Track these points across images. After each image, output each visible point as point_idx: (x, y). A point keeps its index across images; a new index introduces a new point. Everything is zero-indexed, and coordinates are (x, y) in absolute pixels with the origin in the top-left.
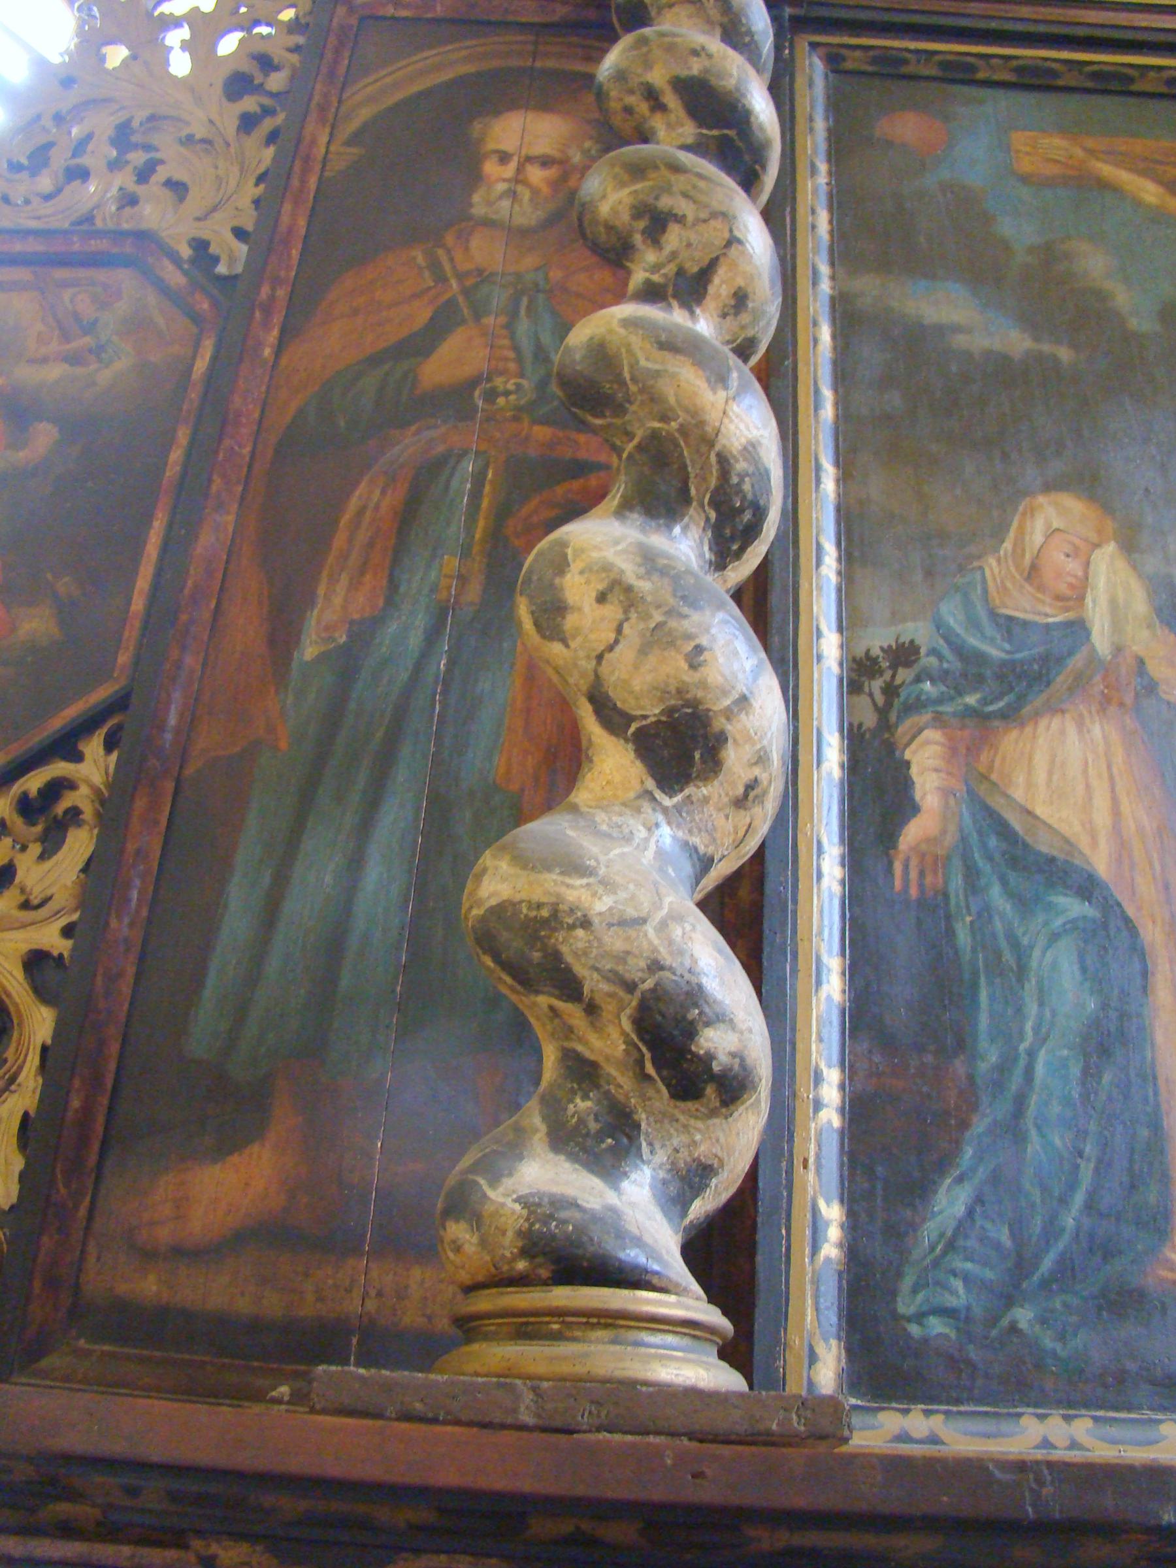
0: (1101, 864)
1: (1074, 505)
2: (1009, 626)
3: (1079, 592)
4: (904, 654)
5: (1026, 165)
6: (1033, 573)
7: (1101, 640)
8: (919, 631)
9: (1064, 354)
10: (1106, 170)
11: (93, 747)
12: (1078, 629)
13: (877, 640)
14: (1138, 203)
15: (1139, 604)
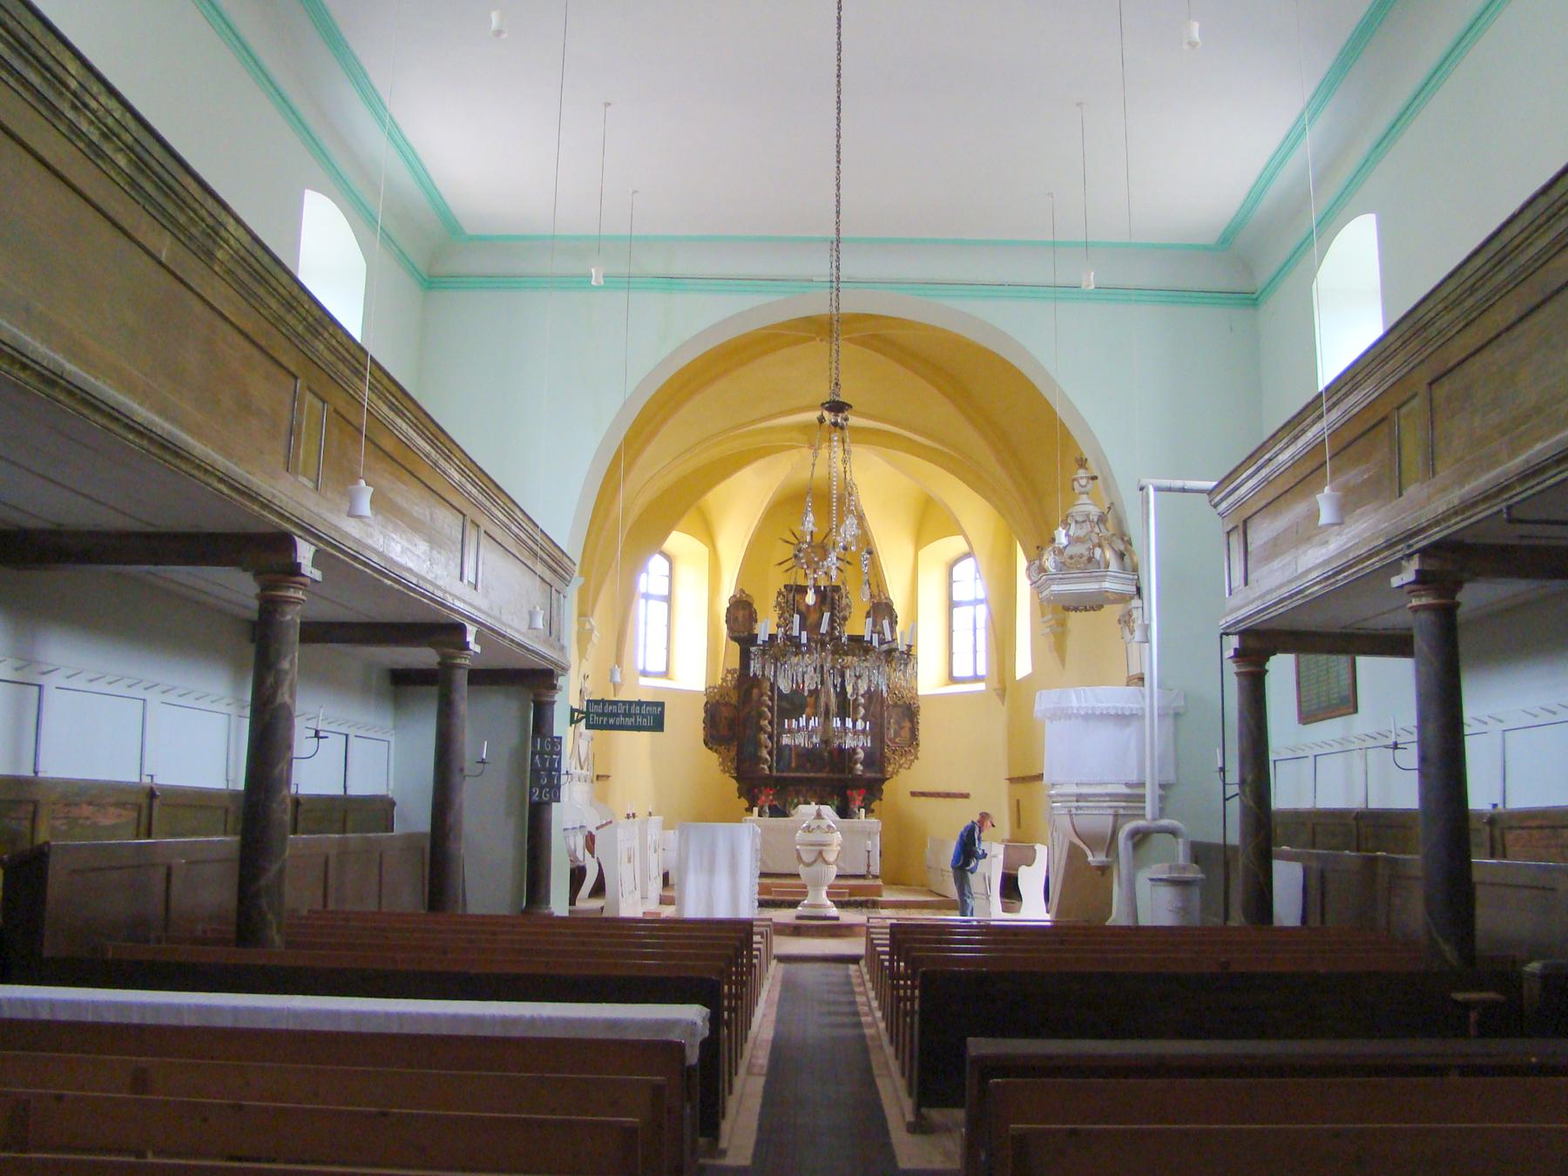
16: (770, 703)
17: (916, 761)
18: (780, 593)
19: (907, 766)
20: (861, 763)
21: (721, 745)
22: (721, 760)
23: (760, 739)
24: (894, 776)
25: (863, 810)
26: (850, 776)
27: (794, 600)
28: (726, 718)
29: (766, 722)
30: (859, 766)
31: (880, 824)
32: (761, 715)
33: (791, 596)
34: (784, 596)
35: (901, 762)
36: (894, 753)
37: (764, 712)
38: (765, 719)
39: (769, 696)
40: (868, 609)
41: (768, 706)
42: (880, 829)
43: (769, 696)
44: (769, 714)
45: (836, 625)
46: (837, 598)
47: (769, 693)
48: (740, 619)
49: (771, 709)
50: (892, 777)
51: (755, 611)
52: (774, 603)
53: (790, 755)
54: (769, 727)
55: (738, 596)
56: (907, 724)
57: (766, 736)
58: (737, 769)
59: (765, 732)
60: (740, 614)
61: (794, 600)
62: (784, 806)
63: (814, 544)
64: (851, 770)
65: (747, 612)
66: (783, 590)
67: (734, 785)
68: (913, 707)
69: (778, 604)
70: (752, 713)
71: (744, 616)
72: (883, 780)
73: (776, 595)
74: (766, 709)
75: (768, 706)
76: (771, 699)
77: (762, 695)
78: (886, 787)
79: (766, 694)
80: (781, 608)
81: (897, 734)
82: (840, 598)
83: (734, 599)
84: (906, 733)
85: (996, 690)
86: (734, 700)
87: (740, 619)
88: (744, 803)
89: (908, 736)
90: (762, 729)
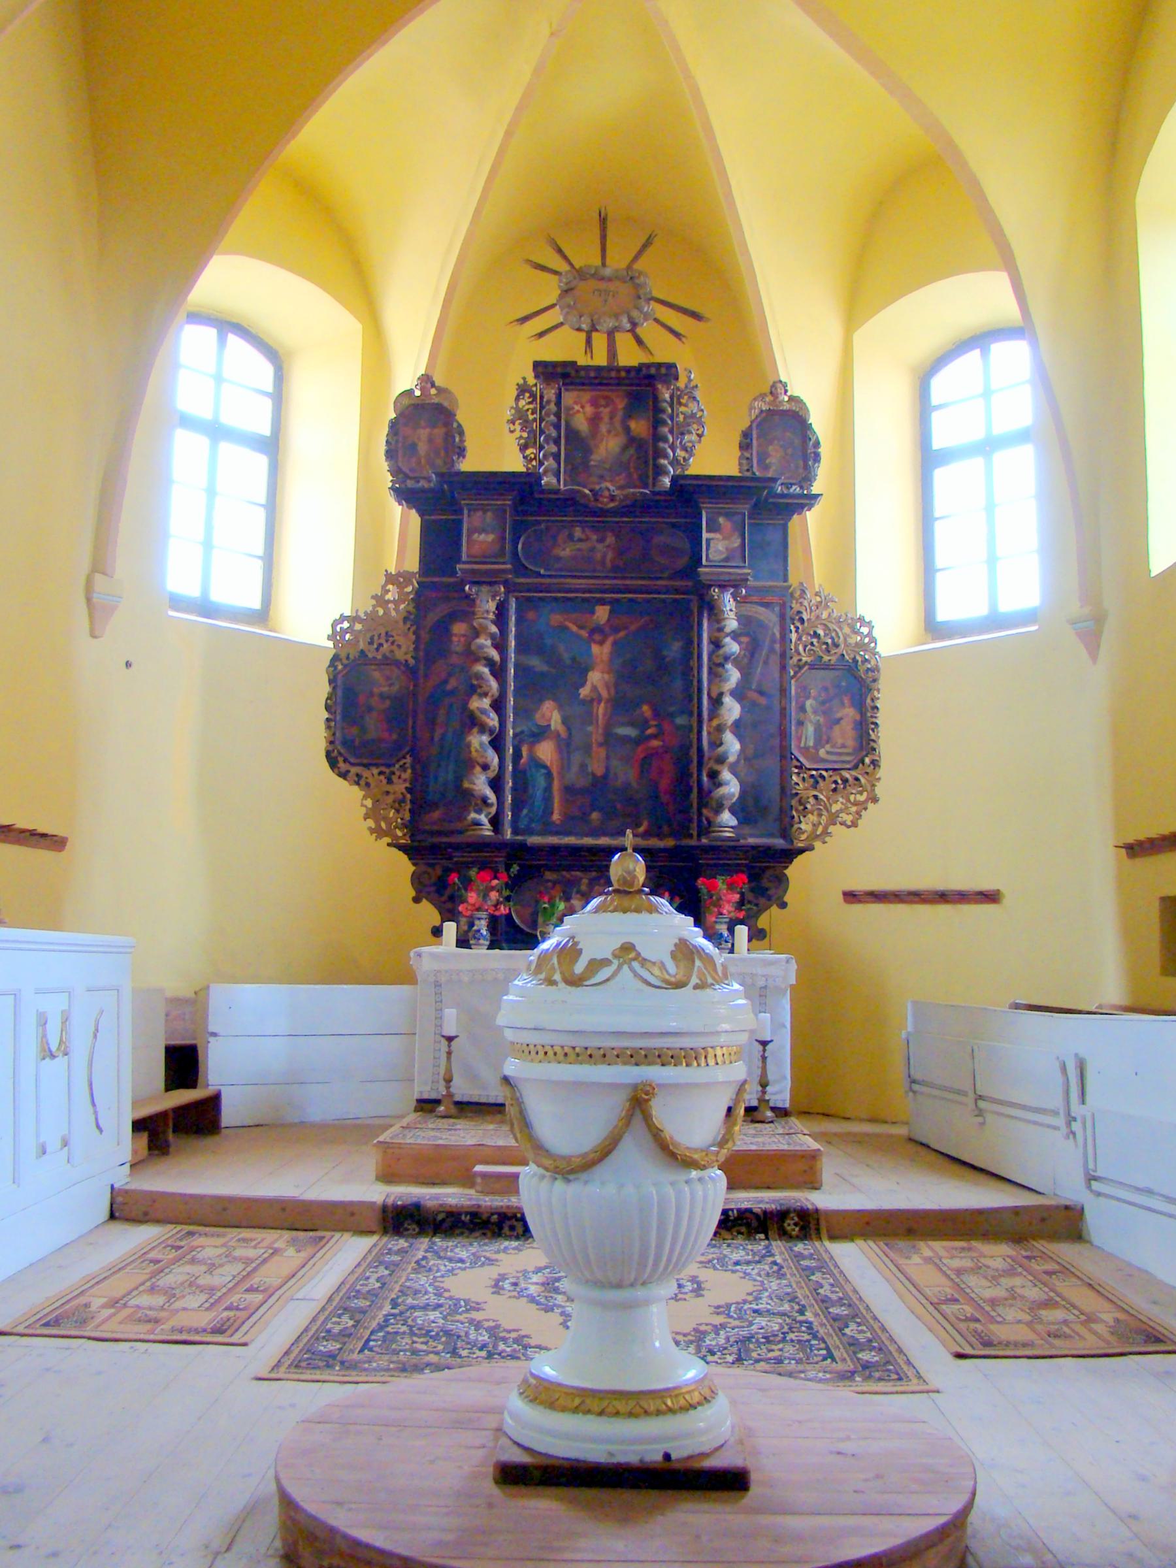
0: (548, 764)
1: (551, 702)
2: (539, 726)
3: (550, 720)
4: (522, 732)
5: (552, 623)
6: (543, 716)
7: (553, 728)
8: (525, 728)
9: (553, 671)
10: (567, 623)
11: (408, 756)
12: (549, 726)
13: (518, 730)
14: (572, 632)
15: (560, 721)
16: (495, 655)
17: (870, 805)
18: (523, 390)
19: (848, 819)
20: (733, 812)
21: (367, 766)
22: (369, 803)
23: (469, 745)
24: (817, 844)
25: (742, 931)
26: (704, 841)
27: (558, 403)
28: (382, 697)
29: (486, 703)
30: (727, 818)
31: (794, 966)
32: (474, 688)
33: (550, 394)
34: (533, 396)
35: (835, 808)
36: (815, 785)
37: (479, 677)
38: (485, 695)
39: (492, 636)
40: (745, 425)
41: (490, 663)
42: (793, 980)
43: (492, 636)
44: (494, 684)
45: (665, 462)
46: (667, 396)
47: (494, 629)
48: (422, 448)
49: (498, 672)
50: (810, 848)
51: (460, 426)
52: (509, 415)
53: (548, 789)
54: (493, 715)
55: (418, 393)
56: (849, 713)
57: (485, 738)
58: (413, 827)
59: (483, 729)
60: (422, 437)
61: (558, 403)
62: (534, 925)
63: (607, 272)
64: (706, 828)
65: (439, 432)
66: (531, 380)
67: (404, 866)
68: (862, 668)
69: (520, 416)
70: (452, 683)
71: (430, 440)
72: (789, 855)
73: (515, 393)
74: (486, 670)
75: (490, 663)
76: (500, 646)
77: (477, 633)
78: (795, 871)
79: (485, 628)
80: (526, 424)
81: (822, 739)
82: (675, 400)
83: (406, 402)
84: (845, 735)
85: (1073, 623)
86: (404, 650)
87: (422, 448)
88: (429, 913)
89: (851, 743)
90: (473, 722)
